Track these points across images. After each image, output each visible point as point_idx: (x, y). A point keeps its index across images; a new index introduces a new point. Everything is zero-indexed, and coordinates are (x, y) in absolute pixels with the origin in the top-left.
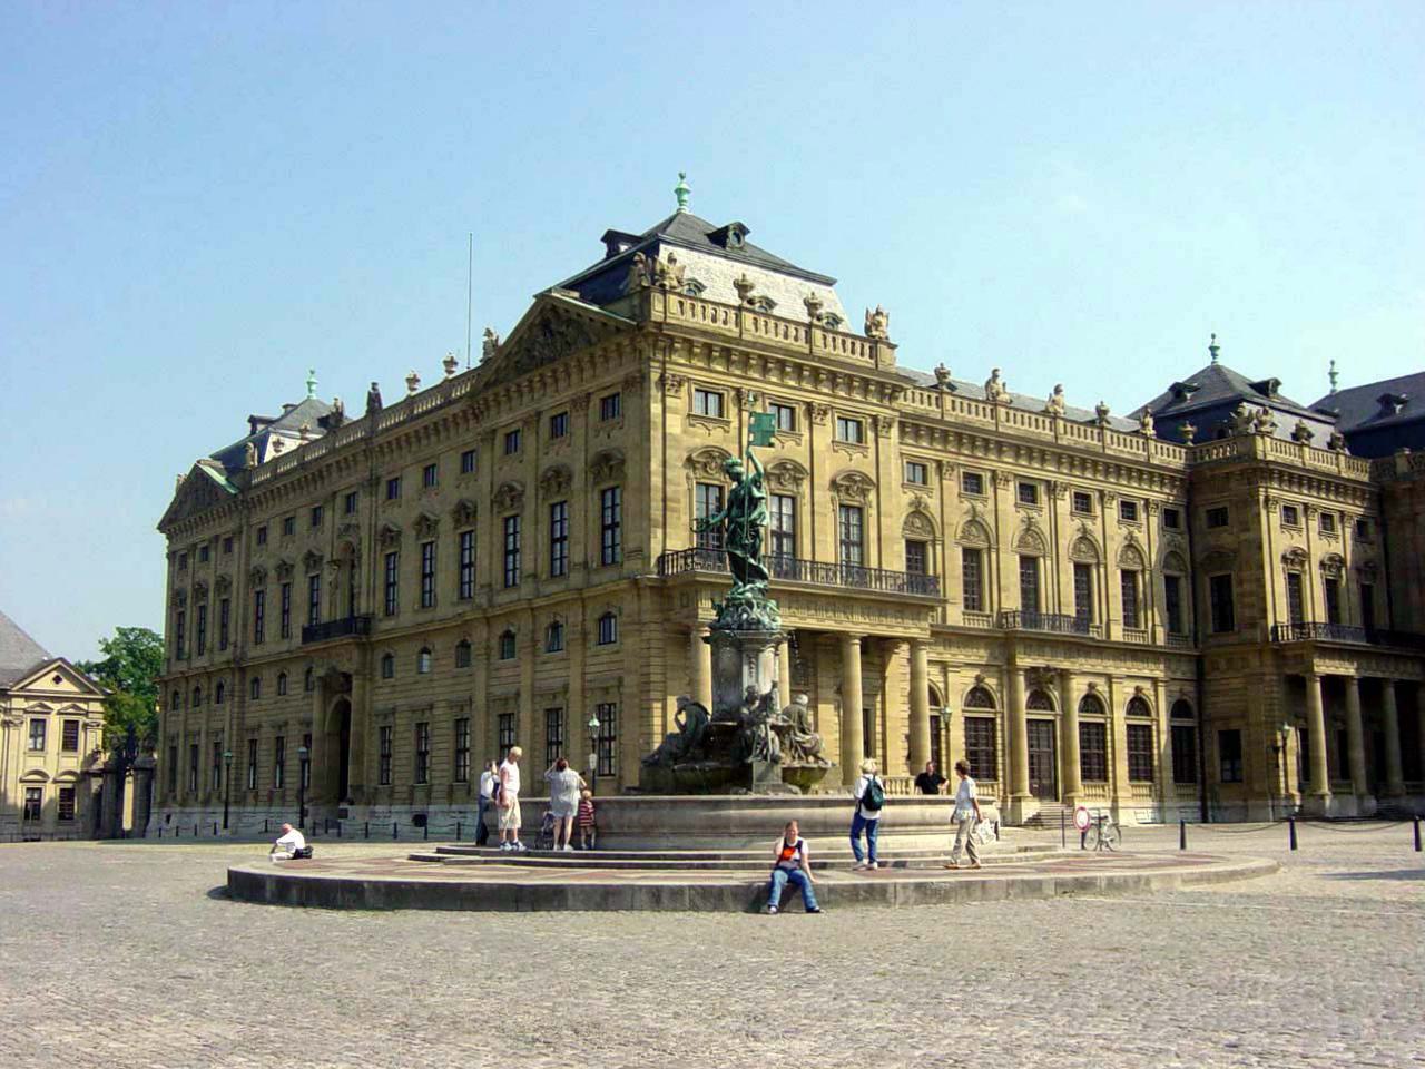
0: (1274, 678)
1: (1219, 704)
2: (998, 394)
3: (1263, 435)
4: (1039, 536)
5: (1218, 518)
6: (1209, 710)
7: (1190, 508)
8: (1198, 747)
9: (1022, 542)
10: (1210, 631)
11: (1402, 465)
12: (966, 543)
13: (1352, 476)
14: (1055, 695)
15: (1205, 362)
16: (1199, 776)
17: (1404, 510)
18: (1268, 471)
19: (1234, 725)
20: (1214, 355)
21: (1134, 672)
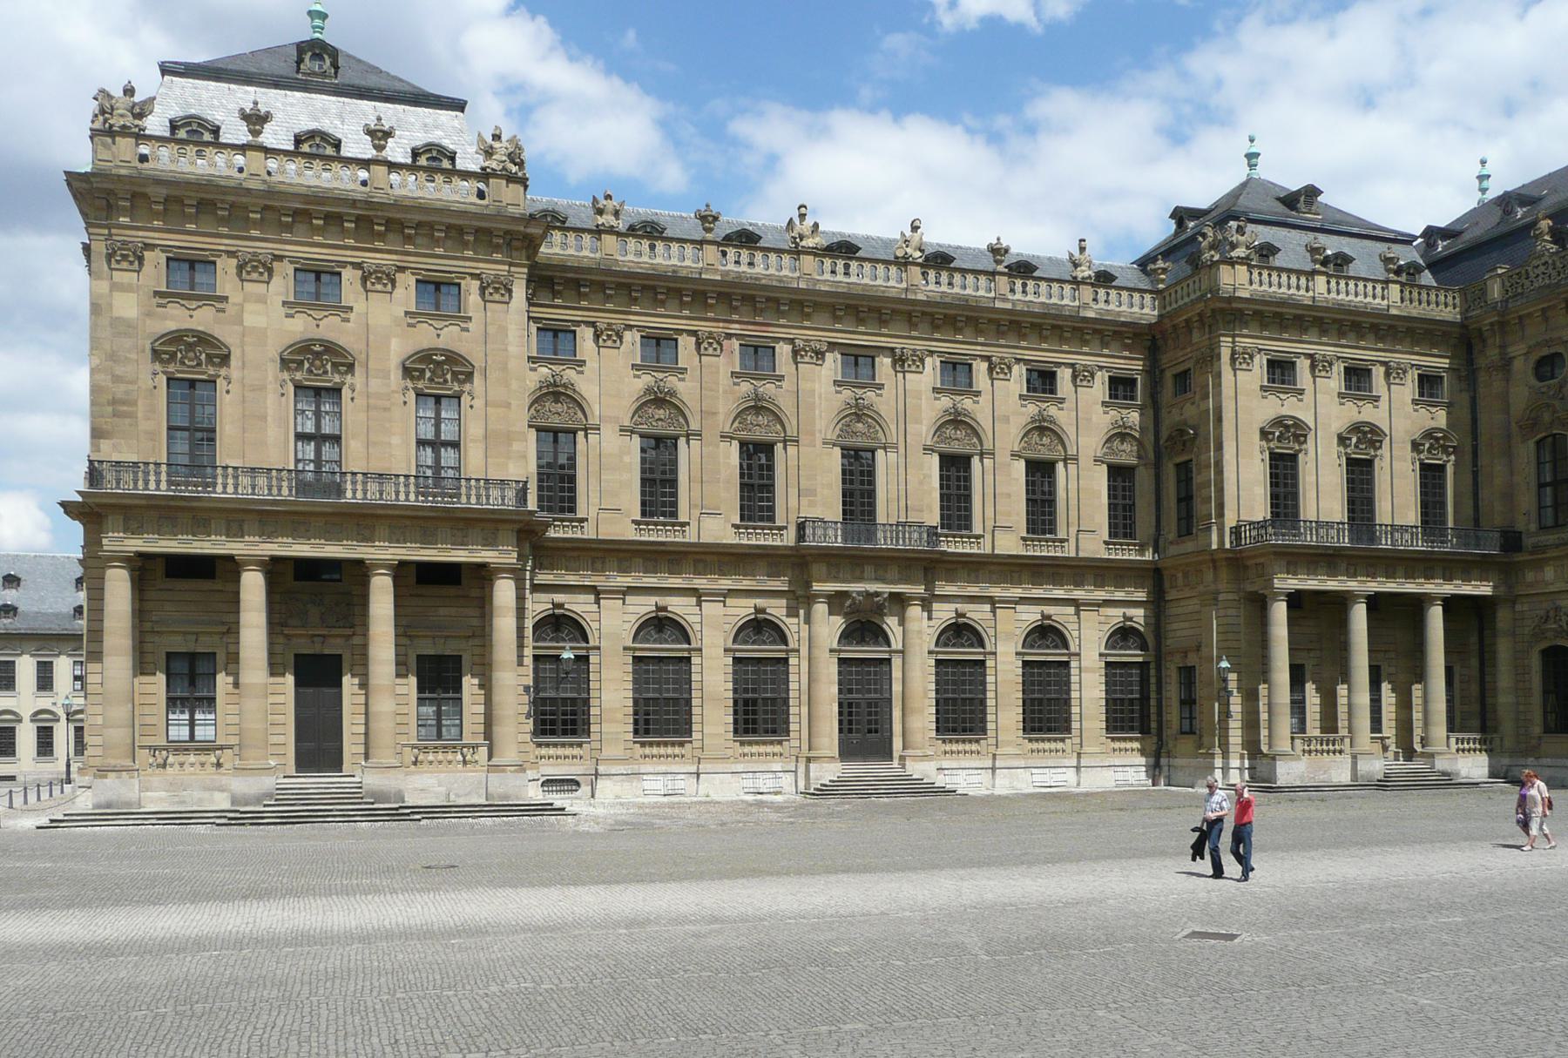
0: (1231, 596)
1: (1179, 632)
2: (802, 237)
3: (1232, 263)
4: (878, 421)
5: (1183, 380)
6: (1170, 643)
7: (1154, 372)
8: (1153, 687)
9: (846, 431)
10: (1172, 536)
11: (1495, 291)
12: (744, 435)
13: (1415, 310)
14: (891, 623)
15: (1236, 175)
16: (1154, 725)
17: (1493, 353)
18: (1236, 314)
19: (1192, 660)
20: (1252, 166)
21: (1038, 592)
